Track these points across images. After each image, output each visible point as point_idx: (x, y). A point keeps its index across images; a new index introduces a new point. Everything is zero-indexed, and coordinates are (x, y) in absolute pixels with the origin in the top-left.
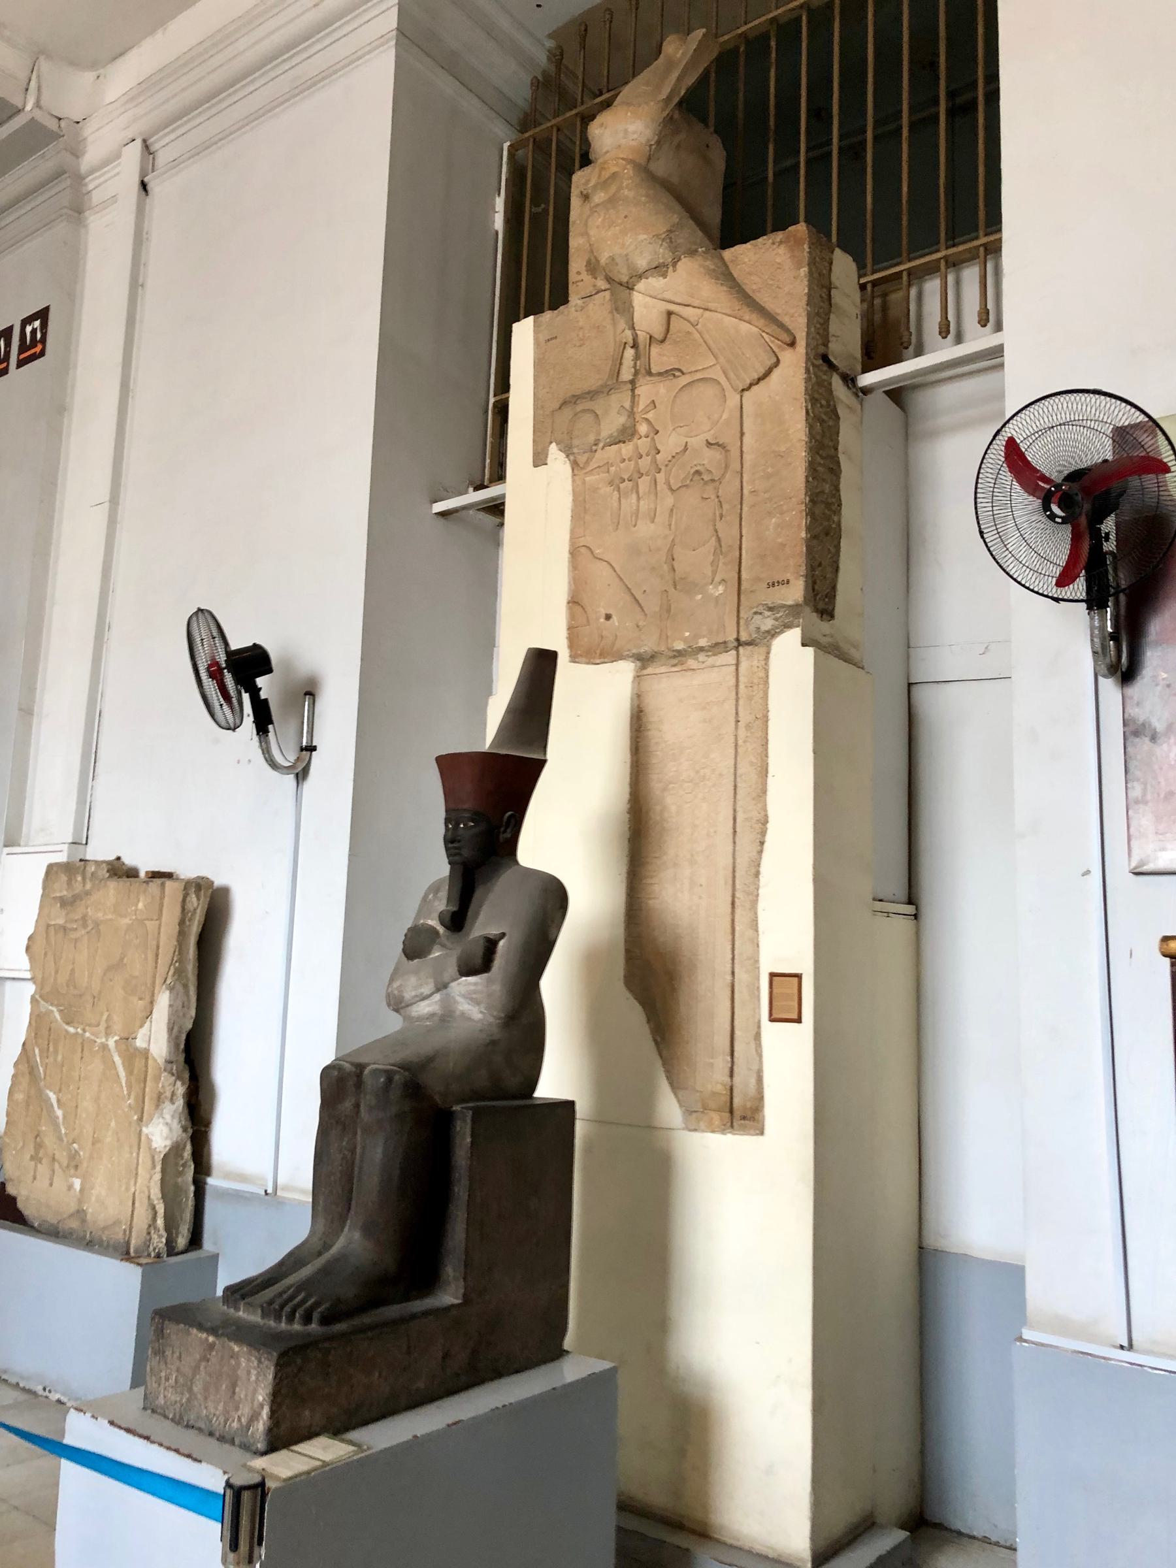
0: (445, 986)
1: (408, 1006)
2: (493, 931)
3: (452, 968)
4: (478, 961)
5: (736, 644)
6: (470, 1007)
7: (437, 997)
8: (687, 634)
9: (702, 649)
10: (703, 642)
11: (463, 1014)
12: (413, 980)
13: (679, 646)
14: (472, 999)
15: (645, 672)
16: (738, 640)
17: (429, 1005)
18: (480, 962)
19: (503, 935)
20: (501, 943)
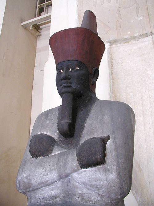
0: (67, 176)
1: (34, 190)
2: (100, 134)
3: (73, 160)
4: (99, 156)
5: (151, 34)
6: (89, 191)
7: (59, 183)
8: (129, 33)
9: (136, 37)
10: (136, 35)
11: (82, 196)
12: (40, 171)
13: (126, 37)
14: (91, 186)
15: (112, 46)
16: (151, 32)
17: (52, 190)
18: (93, 158)
19: (108, 138)
20: (108, 143)
